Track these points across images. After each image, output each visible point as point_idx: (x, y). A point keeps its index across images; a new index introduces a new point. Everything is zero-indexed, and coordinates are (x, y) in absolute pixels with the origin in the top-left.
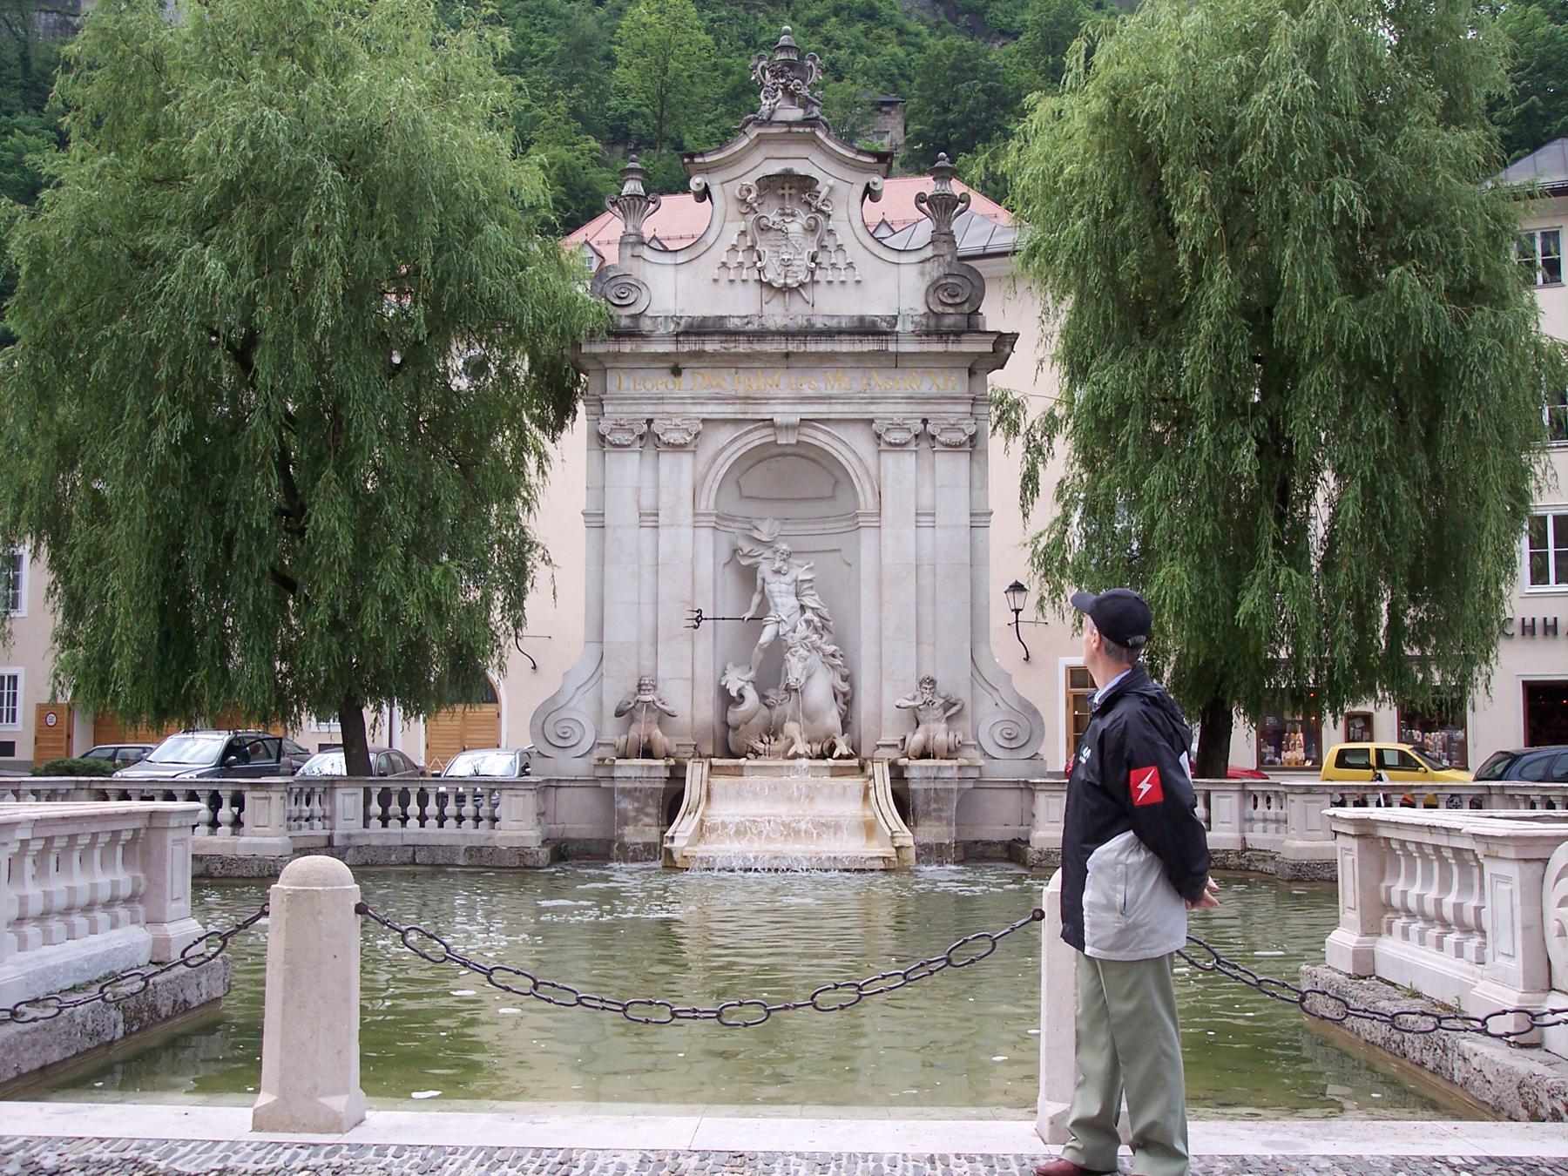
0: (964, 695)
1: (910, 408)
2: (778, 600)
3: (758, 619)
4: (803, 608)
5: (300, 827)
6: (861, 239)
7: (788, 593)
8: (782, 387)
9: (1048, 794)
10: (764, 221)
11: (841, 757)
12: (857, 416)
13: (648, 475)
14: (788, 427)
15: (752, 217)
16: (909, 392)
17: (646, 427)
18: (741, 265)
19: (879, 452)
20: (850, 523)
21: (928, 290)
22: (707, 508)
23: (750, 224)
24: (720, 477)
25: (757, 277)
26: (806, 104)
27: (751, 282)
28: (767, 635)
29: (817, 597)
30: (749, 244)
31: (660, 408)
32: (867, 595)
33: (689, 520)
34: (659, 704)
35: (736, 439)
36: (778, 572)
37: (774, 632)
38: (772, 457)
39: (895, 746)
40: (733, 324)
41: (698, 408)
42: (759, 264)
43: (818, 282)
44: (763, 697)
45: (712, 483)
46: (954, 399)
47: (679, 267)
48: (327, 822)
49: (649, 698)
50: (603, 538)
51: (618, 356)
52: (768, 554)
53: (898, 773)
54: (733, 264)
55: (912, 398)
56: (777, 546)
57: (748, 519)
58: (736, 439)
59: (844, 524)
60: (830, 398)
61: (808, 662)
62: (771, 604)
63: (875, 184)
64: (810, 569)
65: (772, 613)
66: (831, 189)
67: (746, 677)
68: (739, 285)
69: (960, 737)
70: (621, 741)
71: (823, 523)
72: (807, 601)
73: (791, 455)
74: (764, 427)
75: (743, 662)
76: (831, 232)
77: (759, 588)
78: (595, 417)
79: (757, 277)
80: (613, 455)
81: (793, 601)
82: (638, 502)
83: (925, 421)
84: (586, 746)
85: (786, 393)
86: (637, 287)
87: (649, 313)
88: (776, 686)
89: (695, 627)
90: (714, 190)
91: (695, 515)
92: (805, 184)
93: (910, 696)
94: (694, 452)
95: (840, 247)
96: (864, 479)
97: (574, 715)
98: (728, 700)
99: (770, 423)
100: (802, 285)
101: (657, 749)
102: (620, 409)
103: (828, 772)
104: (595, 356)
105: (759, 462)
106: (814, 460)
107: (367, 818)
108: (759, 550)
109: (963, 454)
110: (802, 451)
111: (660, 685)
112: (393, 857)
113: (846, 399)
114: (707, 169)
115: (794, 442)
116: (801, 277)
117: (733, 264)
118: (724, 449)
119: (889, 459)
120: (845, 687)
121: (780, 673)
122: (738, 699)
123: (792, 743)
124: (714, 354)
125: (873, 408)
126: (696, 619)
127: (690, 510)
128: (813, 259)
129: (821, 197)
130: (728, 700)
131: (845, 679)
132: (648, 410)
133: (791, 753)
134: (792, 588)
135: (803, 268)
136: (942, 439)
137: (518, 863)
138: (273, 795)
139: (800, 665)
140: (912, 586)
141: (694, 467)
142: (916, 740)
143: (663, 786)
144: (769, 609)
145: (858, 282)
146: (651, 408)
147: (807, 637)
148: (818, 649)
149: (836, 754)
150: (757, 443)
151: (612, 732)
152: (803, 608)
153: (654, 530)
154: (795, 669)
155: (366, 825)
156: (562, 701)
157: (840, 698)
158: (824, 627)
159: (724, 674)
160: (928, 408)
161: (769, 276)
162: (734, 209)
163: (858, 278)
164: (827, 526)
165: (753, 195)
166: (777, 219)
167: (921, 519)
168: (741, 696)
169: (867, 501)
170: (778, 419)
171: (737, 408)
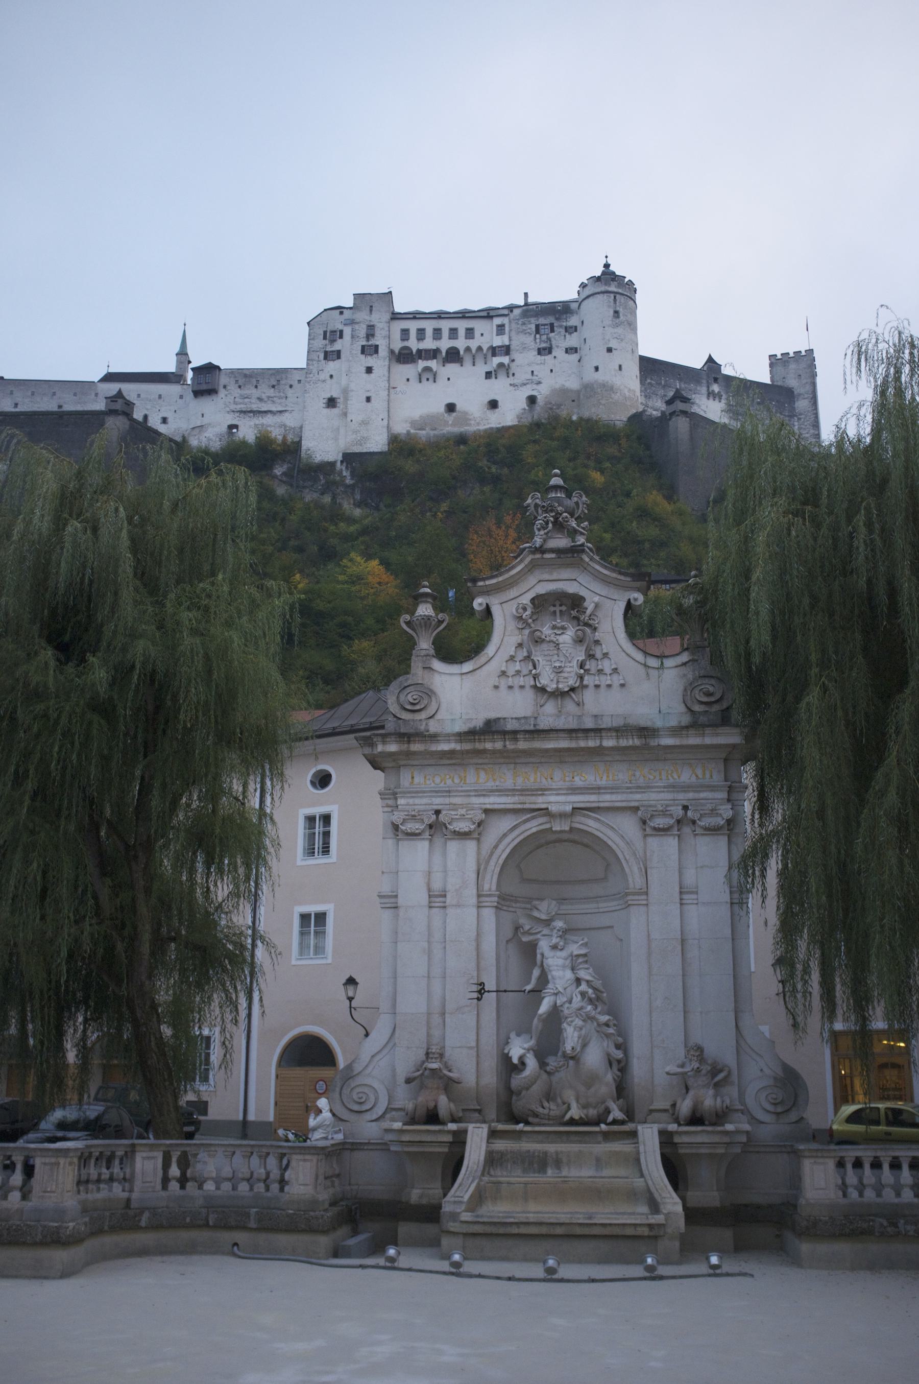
0: (729, 1059)
1: (670, 796)
2: (554, 973)
3: (537, 992)
4: (578, 981)
5: (98, 1190)
6: (625, 647)
7: (564, 967)
8: (556, 779)
9: (812, 1160)
10: (538, 633)
11: (615, 1122)
12: (624, 804)
13: (437, 859)
14: (562, 816)
15: (527, 632)
16: (671, 780)
17: (434, 817)
18: (518, 672)
19: (645, 836)
20: (621, 902)
21: (685, 690)
22: (490, 890)
23: (525, 637)
24: (501, 862)
25: (532, 683)
26: (573, 533)
27: (528, 688)
28: (544, 1008)
30: (525, 654)
31: (447, 800)
32: (637, 969)
33: (474, 900)
34: (446, 1072)
36: (554, 947)
37: (552, 1003)
38: (548, 843)
39: (665, 1111)
40: (510, 726)
41: (482, 800)
42: (534, 672)
43: (587, 686)
44: (542, 1064)
45: (494, 867)
46: (712, 788)
47: (464, 677)
48: (127, 1185)
49: (434, 1066)
50: (396, 917)
51: (409, 754)
53: (666, 1139)
54: (511, 672)
55: (674, 787)
57: (529, 900)
59: (615, 903)
60: (599, 788)
61: (583, 1032)
62: (550, 977)
63: (636, 600)
64: (585, 945)
65: (550, 986)
66: (597, 606)
67: (526, 1046)
68: (516, 690)
69: (728, 1102)
70: (410, 1106)
71: (597, 902)
72: (582, 974)
73: (565, 841)
74: (541, 816)
75: (523, 1030)
76: (597, 642)
78: (389, 809)
79: (532, 683)
80: (405, 843)
81: (569, 975)
83: (685, 808)
84: (380, 1110)
85: (560, 784)
86: (430, 693)
87: (438, 717)
88: (556, 1055)
89: (479, 999)
90: (496, 611)
91: (479, 896)
92: (575, 603)
93: (679, 1062)
95: (606, 655)
97: (368, 1081)
98: (510, 1068)
99: (545, 812)
100: (573, 689)
101: (443, 1112)
102: (411, 801)
103: (600, 1138)
104: (391, 754)
105: (538, 847)
106: (586, 846)
107: (166, 1180)
109: (721, 837)
111: (447, 1054)
112: (188, 1220)
113: (613, 789)
114: (487, 592)
115: (567, 828)
116: (571, 682)
117: (511, 672)
118: (505, 835)
119: (653, 842)
120: (619, 1054)
122: (520, 1067)
123: (569, 1108)
124: (494, 752)
125: (638, 796)
126: (479, 992)
127: (475, 892)
128: (581, 667)
129: (588, 612)
130: (510, 1068)
131: (618, 1047)
132: (438, 802)
133: (567, 1117)
134: (568, 962)
135: (573, 674)
136: (702, 824)
137: (303, 1226)
138: (62, 1161)
139: (576, 1034)
140: (678, 959)
141: (479, 853)
142: (685, 1107)
144: (547, 982)
145: (622, 685)
146: (438, 801)
147: (581, 1008)
148: (592, 1019)
149: (610, 1118)
150: (534, 830)
151: (404, 1099)
152: (578, 981)
153: (442, 910)
154: (571, 1037)
155: (165, 1187)
156: (358, 1068)
158: (598, 999)
159: (508, 1043)
160: (691, 795)
161: (544, 681)
162: (512, 625)
163: (622, 682)
164: (601, 905)
165: (528, 612)
166: (550, 632)
167: (685, 896)
168: (523, 1063)
169: (635, 880)
170: (553, 808)
171: (516, 799)
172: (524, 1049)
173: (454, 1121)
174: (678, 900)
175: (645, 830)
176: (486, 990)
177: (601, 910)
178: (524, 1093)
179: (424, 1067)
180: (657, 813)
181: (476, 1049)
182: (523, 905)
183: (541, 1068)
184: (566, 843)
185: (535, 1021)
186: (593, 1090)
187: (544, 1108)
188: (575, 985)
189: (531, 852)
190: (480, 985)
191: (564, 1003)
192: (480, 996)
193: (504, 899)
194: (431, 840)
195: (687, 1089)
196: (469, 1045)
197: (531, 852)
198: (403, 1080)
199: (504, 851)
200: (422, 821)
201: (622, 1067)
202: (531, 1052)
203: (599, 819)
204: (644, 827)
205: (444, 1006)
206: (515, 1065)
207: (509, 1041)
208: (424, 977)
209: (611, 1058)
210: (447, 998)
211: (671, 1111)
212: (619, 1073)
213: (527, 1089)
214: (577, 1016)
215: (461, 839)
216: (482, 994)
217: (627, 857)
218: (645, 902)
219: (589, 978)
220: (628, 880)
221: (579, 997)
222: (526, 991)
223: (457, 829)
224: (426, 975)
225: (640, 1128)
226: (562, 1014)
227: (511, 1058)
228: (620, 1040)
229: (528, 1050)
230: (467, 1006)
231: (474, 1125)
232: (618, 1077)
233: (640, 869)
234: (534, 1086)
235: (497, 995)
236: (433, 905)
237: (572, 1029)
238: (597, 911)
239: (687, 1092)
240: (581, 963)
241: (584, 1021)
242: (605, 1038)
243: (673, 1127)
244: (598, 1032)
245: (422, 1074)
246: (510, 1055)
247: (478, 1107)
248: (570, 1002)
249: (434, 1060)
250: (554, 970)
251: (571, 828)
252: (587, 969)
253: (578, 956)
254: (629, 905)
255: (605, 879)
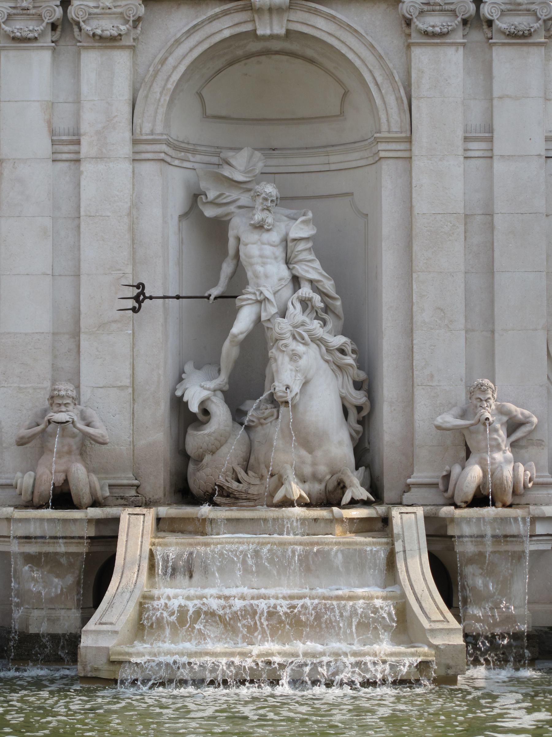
2: (260, 269)
4: (296, 281)
22: (152, 133)
24: (171, 86)
29: (317, 264)
33: (126, 149)
34: (81, 425)
35: (195, 29)
36: (260, 227)
37: (253, 317)
38: (249, 56)
39: (434, 485)
49: (62, 417)
52: (244, 199)
56: (258, 188)
58: (195, 29)
59: (356, 155)
62: (250, 274)
65: (250, 289)
67: (212, 384)
72: (301, 270)
73: (277, 53)
77: (231, 251)
80: (12, 53)
82: (49, 123)
89: (135, 310)
91: (135, 142)
94: (132, 48)
96: (386, 88)
105: (231, 64)
106: (312, 61)
108: (233, 194)
109: (534, 50)
110: (294, 47)
118: (178, 42)
120: (359, 397)
121: (264, 377)
122: (201, 417)
123: (280, 483)
126: (136, 298)
127: (127, 135)
131: (358, 386)
133: (279, 496)
141: (135, 71)
143: (83, 549)
144: (247, 283)
147: (303, 324)
148: (319, 341)
149: (346, 499)
150: (227, 33)
157: (353, 415)
158: (327, 309)
159: (180, 380)
164: (333, 159)
168: (206, 412)
172: (208, 389)
173: (95, 504)
174: (460, 152)
175: (409, 35)
176: (147, 295)
177: (333, 167)
178: (207, 458)
179: (46, 419)
180: (430, 8)
181: (130, 390)
182: (206, 159)
183: (234, 419)
184: (277, 57)
185: (227, 344)
186: (319, 453)
187: (239, 482)
188: (291, 286)
189: (219, 71)
190: (138, 287)
191: (273, 316)
192: (137, 305)
193: (175, 148)
194: (54, 50)
195: (468, 453)
196: (119, 384)
197: (219, 71)
198: (13, 440)
199: (175, 68)
200: (40, 17)
201: (364, 417)
202: (219, 394)
203: (334, 17)
204: (407, 31)
205: (77, 322)
206: (194, 414)
207: (184, 376)
208: (45, 274)
209: (347, 405)
210: (83, 309)
211: (441, 487)
212: (359, 427)
213: (213, 453)
214: (294, 338)
215: (106, 47)
216: (140, 302)
217: (379, 79)
218: (406, 154)
219: (313, 275)
220: (379, 119)
221: (298, 306)
222: (212, 298)
223: (99, 32)
224: (50, 272)
225: (395, 512)
226: (269, 334)
227: (186, 403)
228: (362, 375)
229: (215, 391)
230: (115, 321)
231: (130, 510)
232: (357, 432)
233: (399, 99)
234: (224, 450)
235: (164, 304)
236: (59, 156)
237: (287, 359)
238: (326, 168)
239: (468, 457)
240: (301, 251)
241: (305, 344)
242: (338, 372)
243: (446, 511)
244: (327, 361)
245: (44, 431)
246: (185, 399)
247: (136, 482)
248: (283, 316)
249: (63, 408)
250: (257, 263)
251: (288, 31)
252: (309, 261)
253: (294, 240)
254: (381, 158)
255: (342, 113)
